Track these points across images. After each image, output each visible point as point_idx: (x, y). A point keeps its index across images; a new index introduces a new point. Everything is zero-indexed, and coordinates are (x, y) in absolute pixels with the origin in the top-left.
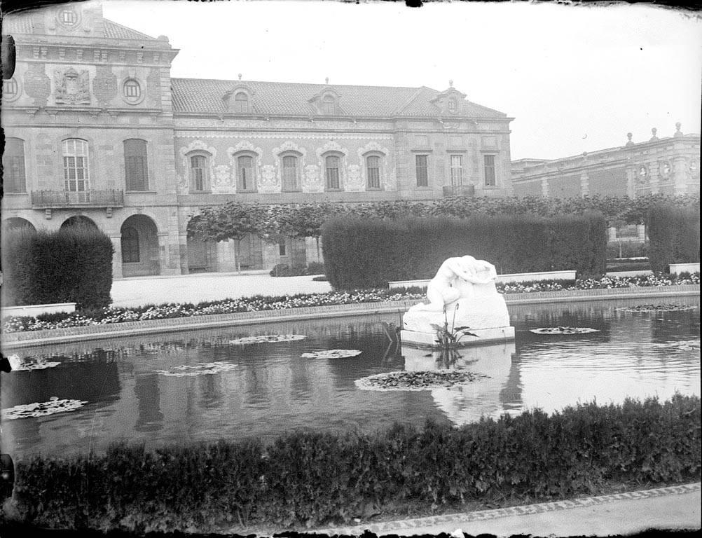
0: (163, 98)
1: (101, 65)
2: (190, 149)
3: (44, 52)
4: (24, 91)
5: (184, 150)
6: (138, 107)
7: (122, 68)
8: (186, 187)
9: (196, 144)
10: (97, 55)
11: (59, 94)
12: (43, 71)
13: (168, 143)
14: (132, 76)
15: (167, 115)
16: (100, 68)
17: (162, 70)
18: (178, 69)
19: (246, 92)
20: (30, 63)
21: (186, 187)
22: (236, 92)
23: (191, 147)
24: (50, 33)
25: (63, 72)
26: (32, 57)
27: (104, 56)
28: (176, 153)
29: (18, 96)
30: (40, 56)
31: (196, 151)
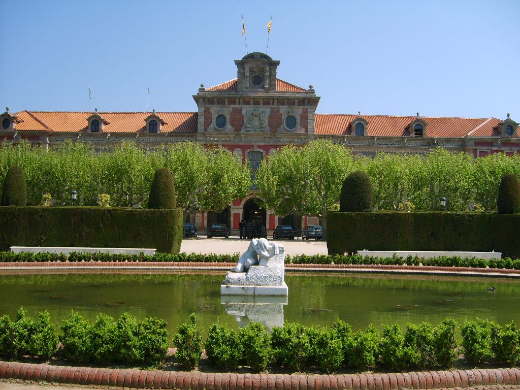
1: (274, 108)
3: (242, 101)
4: (229, 124)
7: (285, 109)
11: (248, 126)
14: (291, 114)
18: (320, 109)
19: (362, 122)
20: (233, 108)
22: (357, 122)
24: (245, 90)
25: (251, 112)
26: (235, 104)
27: (276, 102)
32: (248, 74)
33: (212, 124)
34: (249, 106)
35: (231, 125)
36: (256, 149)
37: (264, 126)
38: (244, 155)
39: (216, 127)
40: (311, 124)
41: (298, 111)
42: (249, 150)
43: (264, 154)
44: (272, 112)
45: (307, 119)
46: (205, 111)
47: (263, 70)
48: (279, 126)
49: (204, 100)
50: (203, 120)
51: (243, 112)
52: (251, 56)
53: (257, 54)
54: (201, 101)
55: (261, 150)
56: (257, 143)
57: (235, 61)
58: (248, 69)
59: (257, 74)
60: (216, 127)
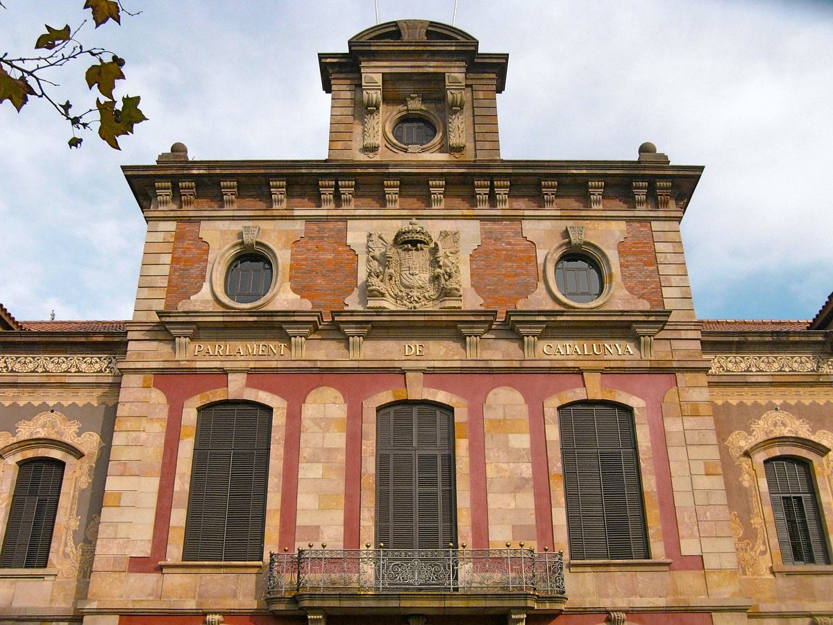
0: (667, 292)
2: (759, 436)
3: (346, 193)
4: (288, 285)
5: (741, 441)
6: (601, 309)
7: (547, 224)
8: (764, 553)
9: (775, 425)
10: (482, 193)
12: (343, 234)
13: (695, 413)
14: (575, 239)
15: (684, 335)
16: (489, 225)
17: (656, 226)
20: (308, 219)
21: (764, 553)
23: (762, 429)
24: (362, 157)
26: (319, 206)
27: (502, 193)
28: (724, 451)
29: (269, 295)
30: (338, 206)
31: (782, 440)
32: (376, 95)
33: (206, 286)
34: (382, 212)
35: (295, 291)
36: (418, 390)
37: (452, 284)
38: (355, 415)
39: (226, 300)
40: (675, 281)
41: (607, 232)
42: (386, 397)
43: (461, 416)
44: (487, 235)
45: (655, 262)
46: (179, 237)
47: (433, 87)
48: (527, 291)
49: (175, 188)
50: (166, 270)
51: (356, 235)
52: (391, 32)
53: (412, 24)
54: (164, 194)
55: (441, 397)
56: (423, 365)
57: (321, 56)
58: (378, 78)
59: (415, 105)
60: (226, 300)
